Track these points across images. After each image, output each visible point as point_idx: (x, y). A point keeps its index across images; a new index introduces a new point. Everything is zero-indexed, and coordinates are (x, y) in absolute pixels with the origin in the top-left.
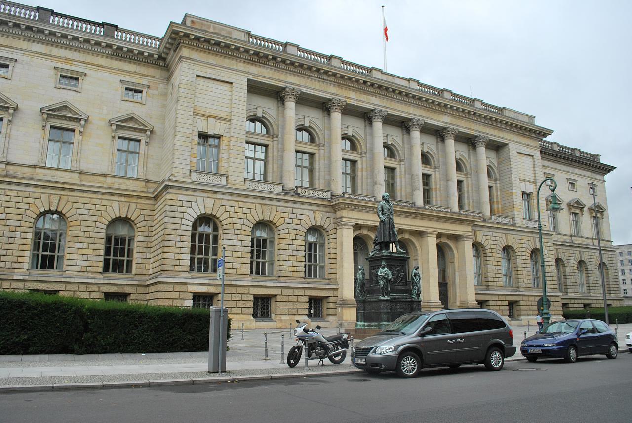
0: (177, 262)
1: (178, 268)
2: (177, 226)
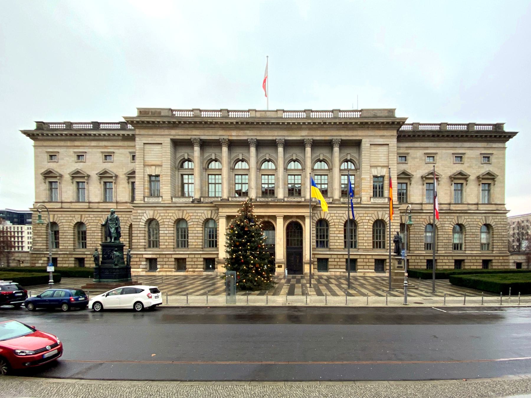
0: (138, 244)
1: (139, 247)
2: (137, 226)
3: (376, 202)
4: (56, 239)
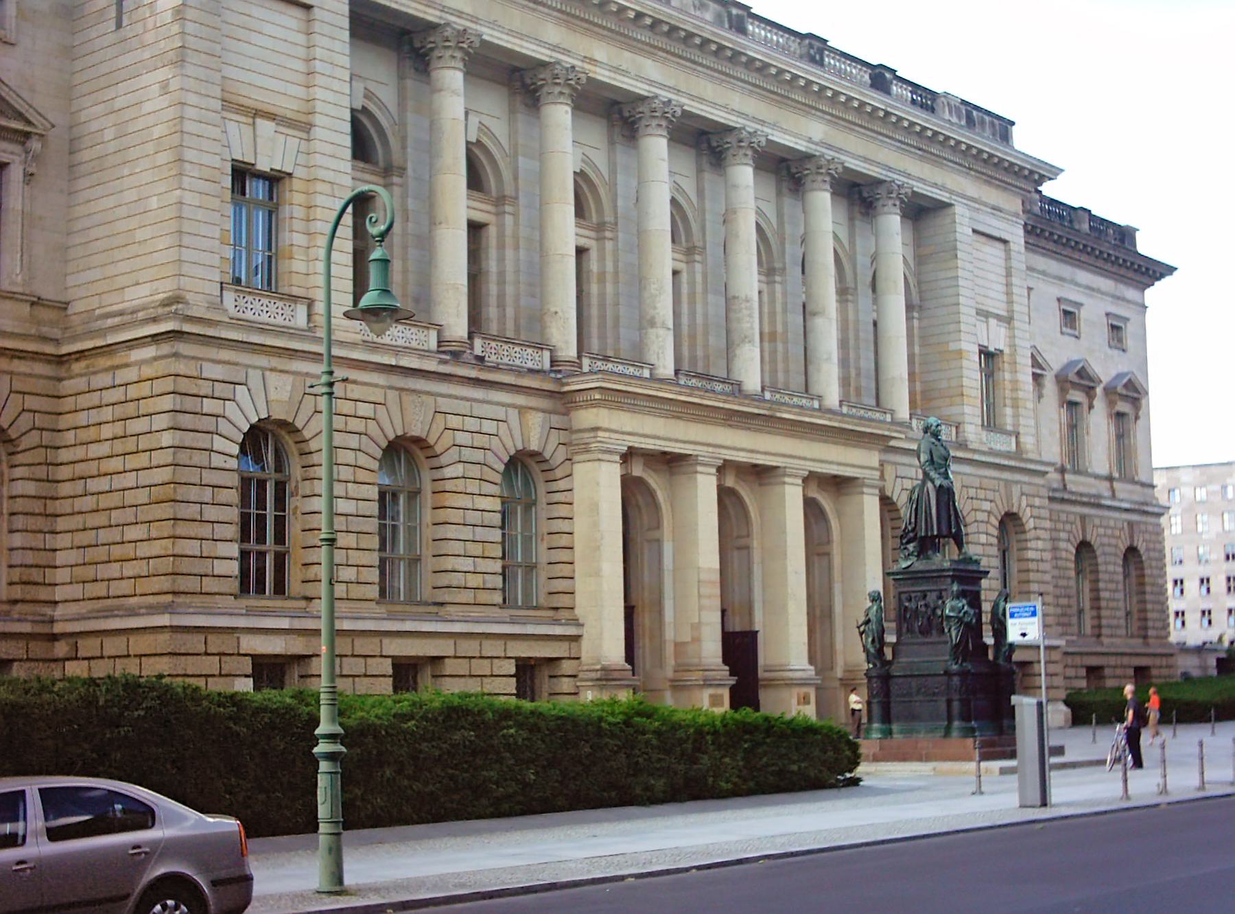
1: (210, 585)
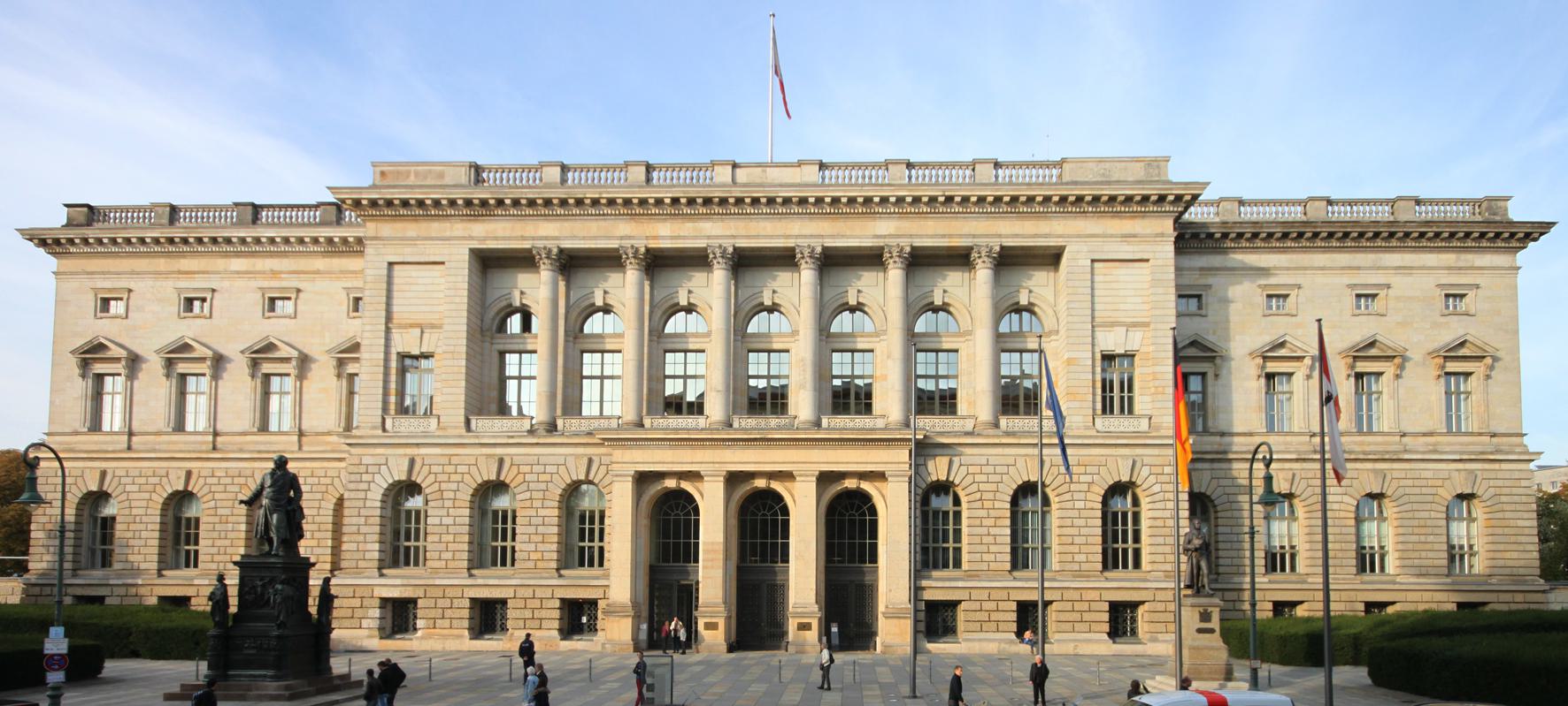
2: (360, 504)
3: (1112, 429)
4: (104, 542)
